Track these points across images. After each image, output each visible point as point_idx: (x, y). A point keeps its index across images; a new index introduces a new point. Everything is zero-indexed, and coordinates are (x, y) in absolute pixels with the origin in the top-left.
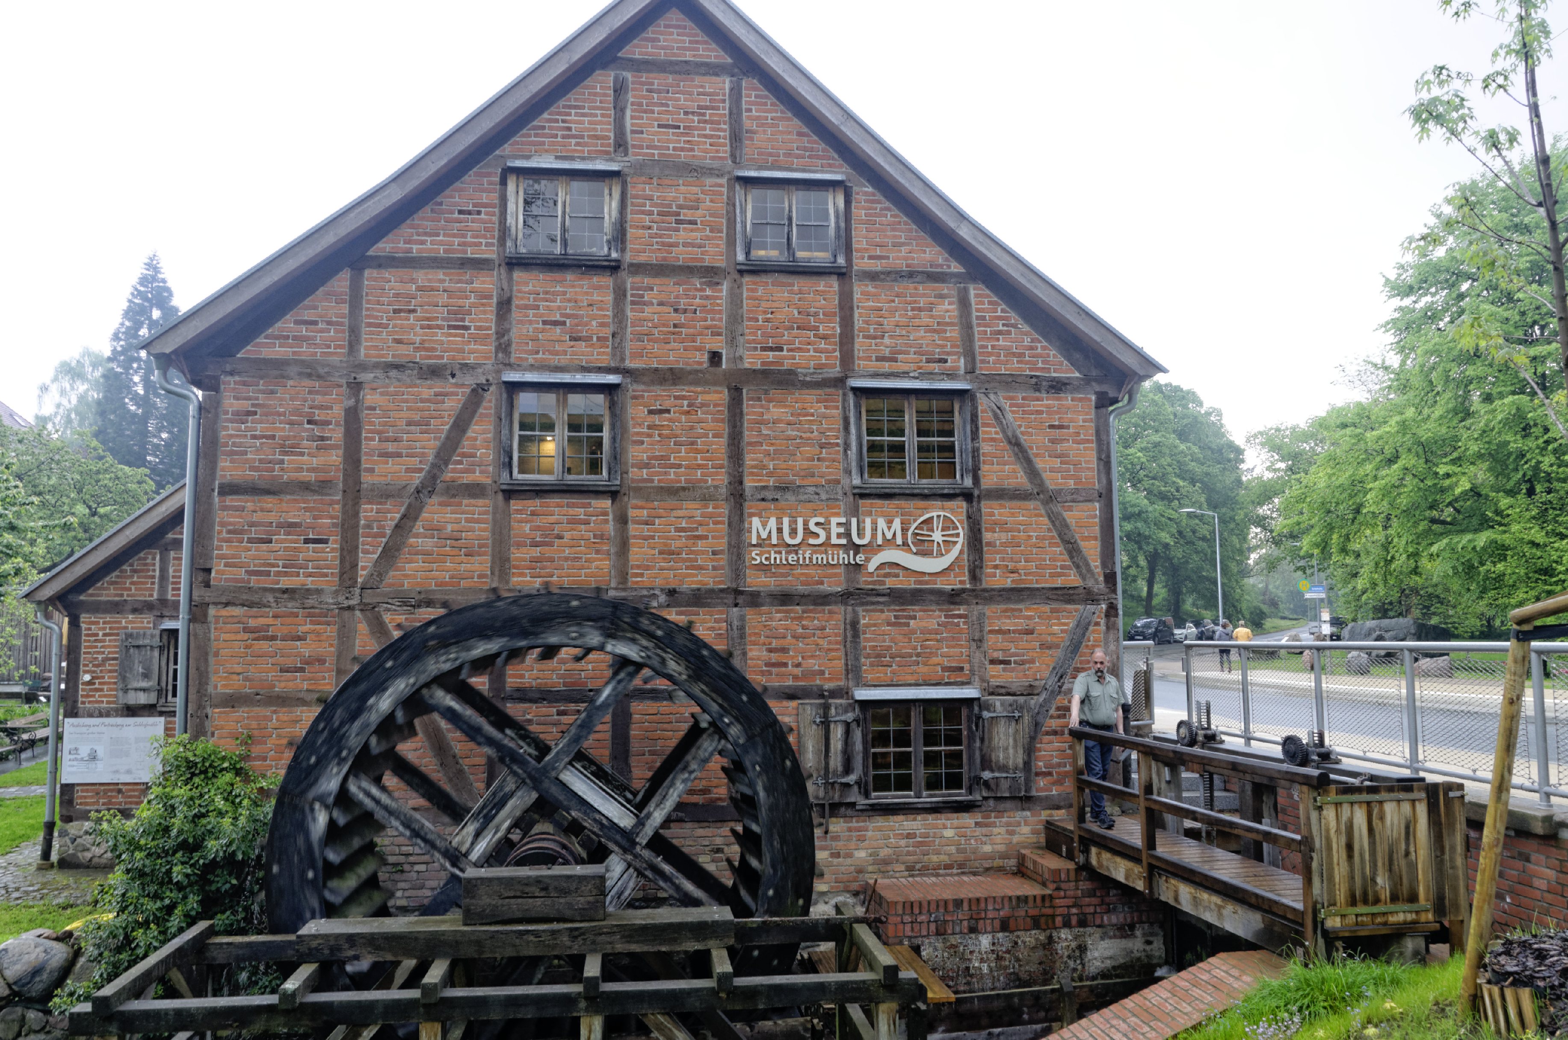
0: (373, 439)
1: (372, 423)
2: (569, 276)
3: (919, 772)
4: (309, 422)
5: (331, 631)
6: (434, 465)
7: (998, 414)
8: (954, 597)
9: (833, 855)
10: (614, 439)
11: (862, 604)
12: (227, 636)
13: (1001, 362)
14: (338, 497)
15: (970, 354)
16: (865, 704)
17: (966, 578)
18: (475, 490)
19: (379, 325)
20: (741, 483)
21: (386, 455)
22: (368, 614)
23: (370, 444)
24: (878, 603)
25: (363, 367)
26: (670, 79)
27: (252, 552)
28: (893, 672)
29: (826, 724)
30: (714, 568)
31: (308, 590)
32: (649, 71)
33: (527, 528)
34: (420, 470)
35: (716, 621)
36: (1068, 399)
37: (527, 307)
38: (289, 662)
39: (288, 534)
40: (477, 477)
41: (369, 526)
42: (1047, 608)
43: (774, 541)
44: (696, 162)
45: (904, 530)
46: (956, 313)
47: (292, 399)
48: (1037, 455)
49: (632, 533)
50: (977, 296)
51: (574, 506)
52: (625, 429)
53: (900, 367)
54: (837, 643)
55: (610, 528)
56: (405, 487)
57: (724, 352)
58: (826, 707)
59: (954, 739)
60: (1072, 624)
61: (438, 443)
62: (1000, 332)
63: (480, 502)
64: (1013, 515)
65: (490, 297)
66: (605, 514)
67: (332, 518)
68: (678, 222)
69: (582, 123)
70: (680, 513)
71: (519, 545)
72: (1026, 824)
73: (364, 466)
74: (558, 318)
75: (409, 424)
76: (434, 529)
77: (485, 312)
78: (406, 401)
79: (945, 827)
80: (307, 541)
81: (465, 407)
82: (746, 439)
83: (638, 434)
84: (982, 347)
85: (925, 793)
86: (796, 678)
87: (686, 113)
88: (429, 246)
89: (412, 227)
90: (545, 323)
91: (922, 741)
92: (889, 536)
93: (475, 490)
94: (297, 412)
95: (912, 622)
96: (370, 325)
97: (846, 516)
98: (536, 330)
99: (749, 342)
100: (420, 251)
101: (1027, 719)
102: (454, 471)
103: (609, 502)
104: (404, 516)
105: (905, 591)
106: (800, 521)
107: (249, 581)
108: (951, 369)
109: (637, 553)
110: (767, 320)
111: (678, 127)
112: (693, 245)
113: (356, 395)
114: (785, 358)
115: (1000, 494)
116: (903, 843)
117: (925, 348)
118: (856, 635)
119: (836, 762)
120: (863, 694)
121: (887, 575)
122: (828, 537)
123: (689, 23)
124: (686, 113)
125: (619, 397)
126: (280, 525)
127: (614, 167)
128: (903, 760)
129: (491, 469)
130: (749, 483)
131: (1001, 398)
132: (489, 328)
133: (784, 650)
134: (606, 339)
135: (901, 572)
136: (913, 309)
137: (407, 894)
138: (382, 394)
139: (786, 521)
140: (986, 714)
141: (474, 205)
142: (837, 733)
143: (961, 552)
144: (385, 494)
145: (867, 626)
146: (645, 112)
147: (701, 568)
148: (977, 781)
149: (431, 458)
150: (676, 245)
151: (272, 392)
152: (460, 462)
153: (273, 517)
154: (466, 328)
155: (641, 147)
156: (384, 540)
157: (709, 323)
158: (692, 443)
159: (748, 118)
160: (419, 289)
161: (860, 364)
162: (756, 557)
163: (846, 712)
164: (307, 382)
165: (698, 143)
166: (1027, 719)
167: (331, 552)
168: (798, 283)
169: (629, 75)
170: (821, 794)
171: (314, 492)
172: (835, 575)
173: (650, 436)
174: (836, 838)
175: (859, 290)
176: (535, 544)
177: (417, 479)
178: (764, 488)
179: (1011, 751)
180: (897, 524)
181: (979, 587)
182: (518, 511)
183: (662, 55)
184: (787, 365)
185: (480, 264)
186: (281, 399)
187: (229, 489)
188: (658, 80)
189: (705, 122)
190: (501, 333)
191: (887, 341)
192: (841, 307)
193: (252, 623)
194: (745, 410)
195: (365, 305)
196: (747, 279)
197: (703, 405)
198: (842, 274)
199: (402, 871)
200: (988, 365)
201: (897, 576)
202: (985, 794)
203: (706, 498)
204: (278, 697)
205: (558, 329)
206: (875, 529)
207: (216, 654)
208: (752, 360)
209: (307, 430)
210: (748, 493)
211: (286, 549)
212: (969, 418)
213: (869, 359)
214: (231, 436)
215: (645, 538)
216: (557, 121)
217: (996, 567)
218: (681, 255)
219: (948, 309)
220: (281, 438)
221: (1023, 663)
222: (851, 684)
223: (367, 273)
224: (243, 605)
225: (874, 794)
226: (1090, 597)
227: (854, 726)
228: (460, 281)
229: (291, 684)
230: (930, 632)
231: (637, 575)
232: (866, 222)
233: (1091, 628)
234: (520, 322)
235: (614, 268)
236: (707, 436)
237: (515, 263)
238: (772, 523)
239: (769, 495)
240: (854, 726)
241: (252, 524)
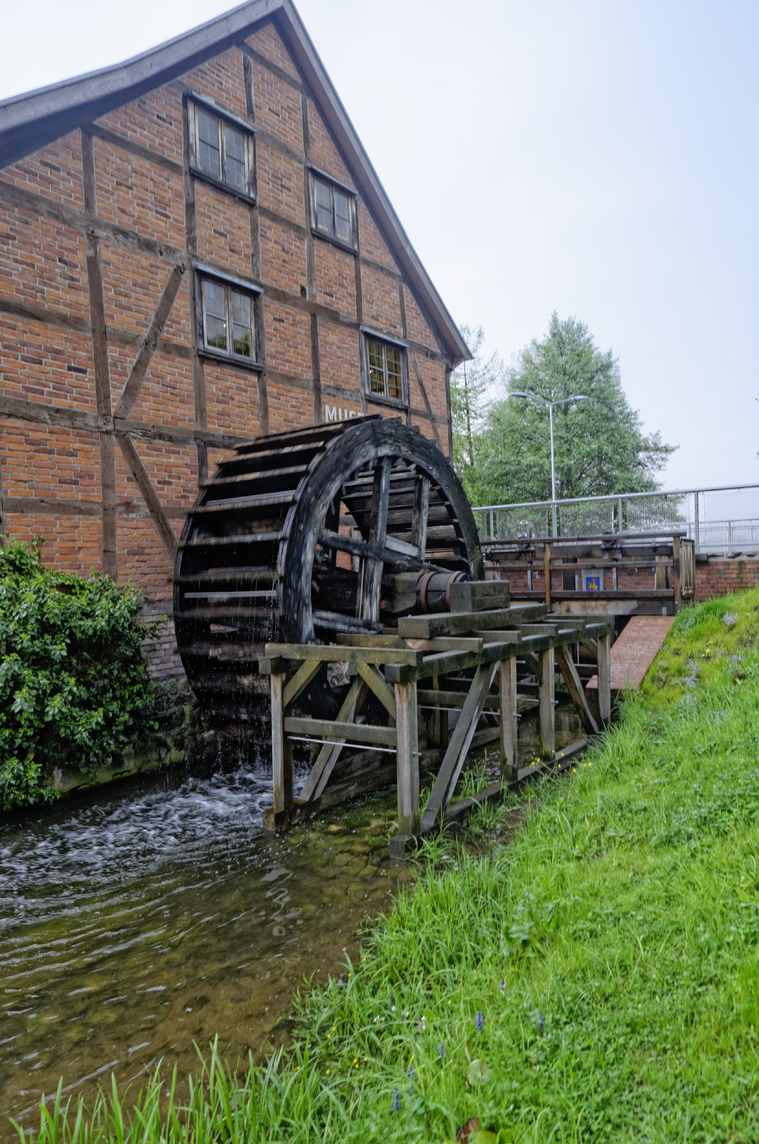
0: (110, 290)
1: (108, 276)
2: (227, 200)
4: (60, 260)
5: (96, 450)
6: (155, 324)
12: (12, 446)
14: (89, 335)
15: (404, 326)
18: (182, 351)
19: (107, 191)
20: (319, 381)
21: (119, 306)
23: (108, 294)
26: (272, 77)
27: (26, 370)
31: (75, 412)
33: (214, 388)
34: (146, 326)
37: (204, 215)
38: (68, 475)
39: (54, 359)
41: (114, 365)
47: (44, 234)
49: (269, 404)
51: (238, 377)
55: (258, 396)
56: (138, 336)
61: (156, 307)
63: (187, 361)
65: (181, 197)
67: (87, 351)
68: (282, 186)
70: (292, 394)
73: (106, 312)
74: (222, 230)
75: (135, 285)
76: (159, 377)
77: (179, 209)
78: (131, 264)
80: (70, 369)
83: (270, 333)
89: (126, 114)
98: (210, 235)
102: (168, 332)
104: (139, 362)
107: (26, 397)
110: (325, 274)
123: (280, 41)
126: (47, 350)
129: (190, 336)
130: (323, 382)
132: (182, 223)
137: (159, 667)
138: (113, 252)
139: (340, 410)
141: (167, 116)
149: (153, 317)
150: (280, 202)
153: (39, 340)
156: (127, 379)
164: (54, 222)
171: (70, 325)
173: (275, 336)
176: (220, 402)
177: (145, 333)
178: (329, 387)
182: (209, 375)
184: (335, 307)
185: (173, 167)
186: (36, 232)
190: (190, 230)
195: (95, 169)
196: (316, 242)
199: (155, 650)
203: (304, 387)
205: (223, 239)
208: (321, 300)
209: (58, 267)
210: (322, 388)
211: (54, 373)
218: (284, 211)
219: (395, 294)
220: (39, 268)
224: (24, 418)
228: (161, 176)
229: (69, 494)
235: (251, 205)
237: (195, 176)
239: (332, 391)
241: (24, 344)
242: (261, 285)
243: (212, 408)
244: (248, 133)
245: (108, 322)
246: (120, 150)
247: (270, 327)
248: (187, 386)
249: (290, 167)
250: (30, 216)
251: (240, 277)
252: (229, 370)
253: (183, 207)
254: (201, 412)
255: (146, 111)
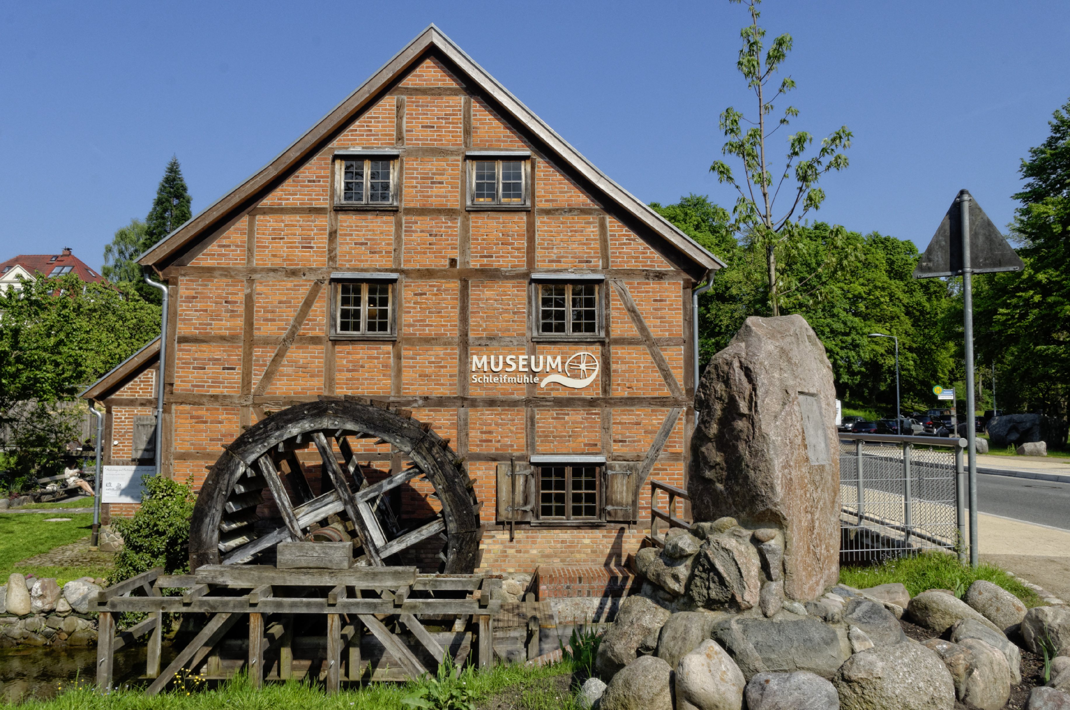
1: (259, 302)
2: (370, 217)
3: (569, 505)
4: (226, 302)
6: (294, 326)
7: (623, 293)
8: (592, 403)
9: (517, 551)
10: (394, 311)
11: (537, 406)
13: (625, 262)
14: (241, 344)
15: (605, 257)
16: (537, 465)
17: (600, 392)
18: (315, 340)
19: (264, 247)
20: (467, 335)
21: (266, 320)
22: (257, 409)
23: (258, 315)
24: (546, 406)
25: (254, 271)
26: (429, 98)
28: (555, 446)
29: (513, 477)
30: (450, 385)
32: (417, 95)
33: (345, 362)
34: (286, 329)
35: (451, 415)
36: (666, 283)
37: (345, 235)
39: (214, 364)
40: (317, 332)
41: (258, 360)
42: (650, 409)
43: (486, 369)
44: (443, 147)
45: (563, 363)
46: (598, 233)
48: (645, 318)
50: (610, 222)
51: (371, 349)
52: (401, 305)
53: (562, 266)
54: (522, 429)
55: (392, 361)
57: (458, 259)
58: (513, 466)
59: (590, 485)
60: (664, 418)
61: (296, 314)
62: (625, 244)
63: (319, 347)
64: (629, 353)
65: (325, 230)
66: (389, 353)
67: (237, 355)
69: (377, 127)
71: (340, 371)
72: (634, 537)
74: (363, 241)
75: (280, 302)
76: (294, 363)
78: (278, 290)
79: (584, 537)
80: (224, 369)
81: (311, 293)
82: (470, 310)
83: (408, 307)
84: (613, 253)
85: (572, 517)
86: (497, 449)
87: (438, 118)
88: (291, 201)
89: (282, 191)
90: (356, 244)
91: (571, 486)
92: (554, 366)
93: (315, 340)
94: (219, 297)
95: (566, 417)
96: (258, 247)
97: (528, 354)
98: (351, 248)
99: (472, 252)
100: (286, 204)
101: (634, 475)
102: (304, 329)
103: (391, 347)
104: (277, 355)
105: (563, 399)
106: (501, 358)
108: (594, 266)
109: (407, 375)
110: (484, 240)
111: (433, 127)
112: (440, 196)
113: (251, 287)
114: (494, 261)
115: (621, 341)
116: (559, 545)
117: (578, 255)
118: (533, 424)
119: (519, 498)
120: (535, 459)
121: (552, 389)
122: (518, 367)
124: (438, 118)
125: (397, 286)
127: (394, 152)
128: (560, 498)
130: (471, 335)
131: (624, 283)
133: (490, 432)
134: (390, 252)
135: (560, 388)
136: (571, 231)
139: (492, 357)
140: (610, 472)
142: (520, 482)
143: (597, 376)
144: (266, 342)
145: (541, 419)
146: (414, 118)
147: (443, 385)
148: (603, 510)
149: (292, 322)
151: (206, 285)
152: (308, 324)
153: (206, 355)
154: (311, 248)
155: (412, 140)
157: (450, 242)
158: (439, 312)
159: (475, 119)
160: (286, 226)
161: (539, 265)
162: (475, 379)
163: (525, 469)
164: (224, 279)
165: (445, 136)
166: (634, 475)
167: (236, 376)
168: (502, 217)
169: (405, 97)
170: (510, 516)
171: (228, 341)
172: (522, 389)
173: (414, 308)
174: (518, 542)
175: (539, 221)
176: (349, 371)
177: (284, 334)
179: (624, 494)
180: (559, 359)
181: (608, 397)
183: (424, 85)
184: (495, 265)
187: (183, 340)
188: (422, 99)
189: (450, 123)
191: (555, 251)
192: (528, 231)
193: (194, 413)
194: (470, 292)
195: (256, 236)
196: (472, 216)
197: (445, 290)
198: (528, 211)
200: (617, 263)
201: (558, 390)
202: (608, 519)
204: (208, 454)
205: (363, 248)
206: (545, 363)
207: (176, 431)
208: (475, 264)
210: (471, 341)
211: (213, 373)
212: (603, 295)
213: (544, 261)
214: (184, 310)
215: (411, 367)
216: (363, 126)
217: (619, 385)
218: (434, 202)
219: (593, 230)
220: (211, 311)
221: (634, 441)
222: (529, 453)
223: (258, 217)
225: (541, 517)
226: (676, 403)
227: (530, 477)
230: (577, 423)
231: (406, 389)
232: (545, 180)
233: (677, 421)
234: (341, 244)
235: (395, 211)
236: (447, 308)
238: (485, 358)
240: (530, 477)
241: (195, 359)
242: (402, 272)
243: (340, 377)
244: (395, 157)
245: (256, 333)
246: (276, 217)
247: (409, 302)
248: (318, 363)
249: (445, 163)
250: (209, 281)
251: (379, 271)
252: (359, 346)
253: (327, 236)
254: (330, 382)
255: (299, 182)
